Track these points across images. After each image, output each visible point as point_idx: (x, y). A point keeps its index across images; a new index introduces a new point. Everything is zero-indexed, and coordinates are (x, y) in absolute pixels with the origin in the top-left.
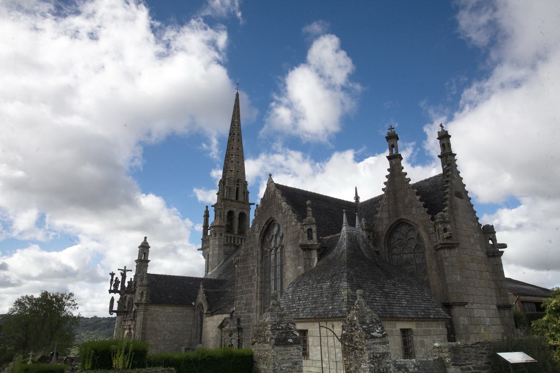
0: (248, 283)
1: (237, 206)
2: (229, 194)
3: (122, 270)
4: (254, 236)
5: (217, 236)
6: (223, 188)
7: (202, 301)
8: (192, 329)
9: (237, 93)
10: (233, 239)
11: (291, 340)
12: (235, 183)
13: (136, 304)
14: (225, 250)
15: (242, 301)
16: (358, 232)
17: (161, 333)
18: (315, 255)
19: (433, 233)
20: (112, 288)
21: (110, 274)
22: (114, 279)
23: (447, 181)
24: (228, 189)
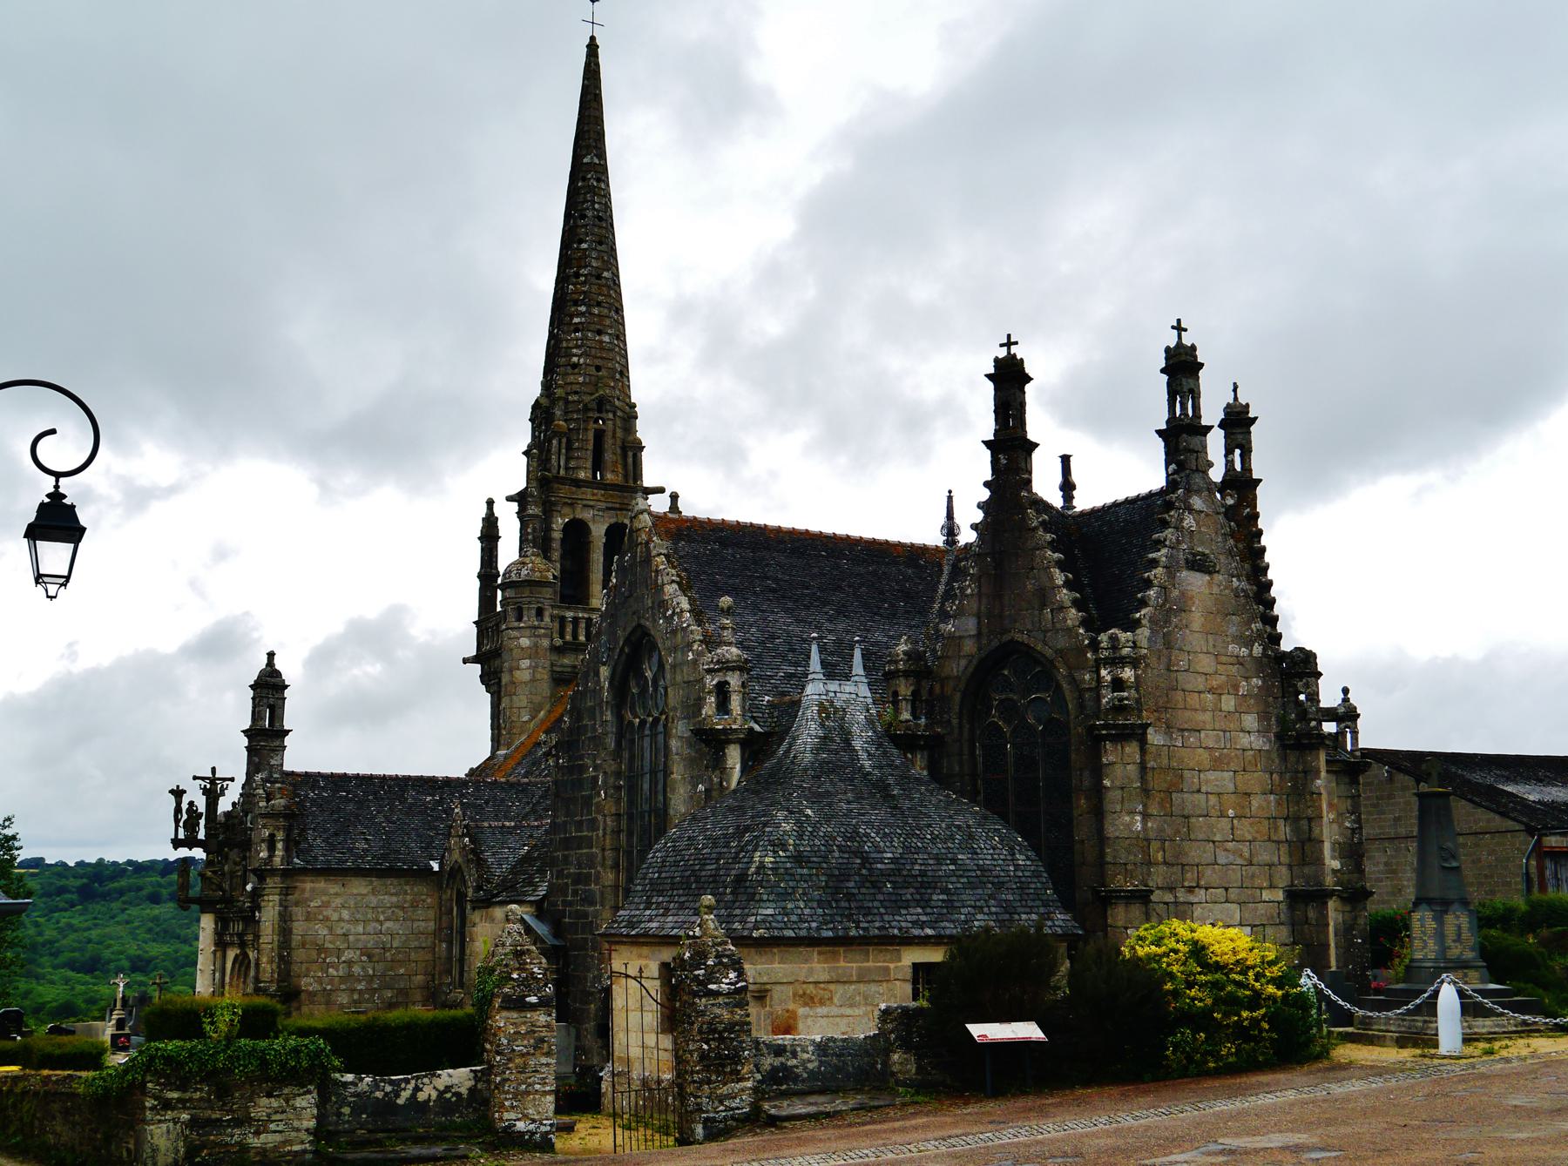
1: (599, 503)
2: (568, 459)
3: (203, 779)
4: (597, 674)
5: (525, 619)
6: (546, 431)
7: (460, 860)
8: (435, 943)
9: (593, 38)
11: (533, 999)
13: (254, 871)
14: (555, 668)
16: (854, 696)
17: (338, 958)
18: (734, 756)
19: (1090, 689)
20: (181, 835)
21: (172, 792)
22: (185, 806)
23: (1165, 524)
24: (564, 440)
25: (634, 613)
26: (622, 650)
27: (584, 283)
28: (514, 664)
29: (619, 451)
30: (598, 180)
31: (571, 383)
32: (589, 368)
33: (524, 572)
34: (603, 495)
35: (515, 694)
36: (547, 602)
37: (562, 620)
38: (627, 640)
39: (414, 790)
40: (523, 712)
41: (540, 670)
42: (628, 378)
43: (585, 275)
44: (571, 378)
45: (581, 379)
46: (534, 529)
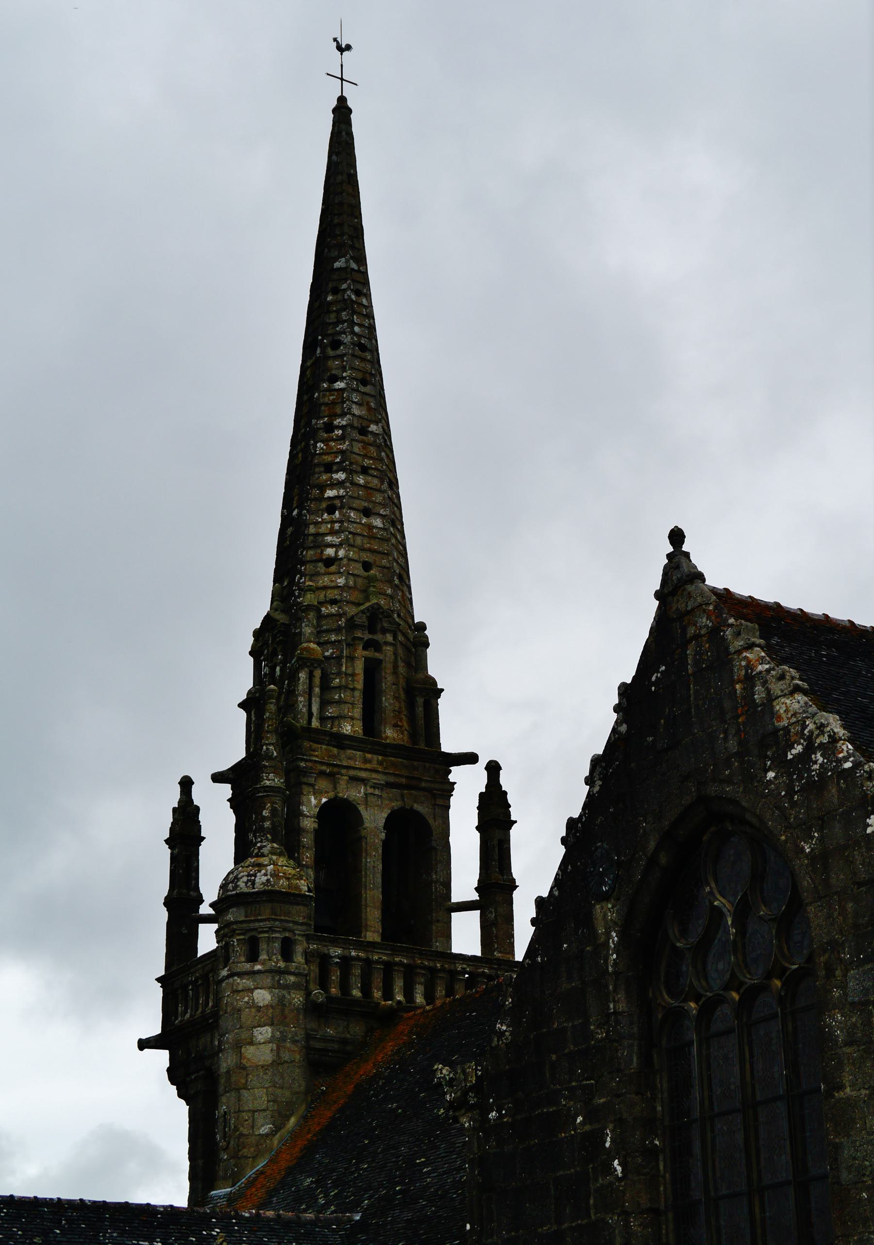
1: (374, 775)
2: (324, 703)
4: (588, 921)
5: (263, 957)
9: (342, 100)
24: (318, 673)
27: (342, 438)
28: (244, 1035)
29: (403, 696)
30: (358, 293)
31: (325, 588)
33: (261, 879)
34: (380, 763)
35: (246, 1088)
36: (299, 930)
37: (324, 960)
40: (260, 1118)
42: (409, 587)
43: (343, 428)
44: (325, 580)
45: (341, 581)
46: (274, 811)
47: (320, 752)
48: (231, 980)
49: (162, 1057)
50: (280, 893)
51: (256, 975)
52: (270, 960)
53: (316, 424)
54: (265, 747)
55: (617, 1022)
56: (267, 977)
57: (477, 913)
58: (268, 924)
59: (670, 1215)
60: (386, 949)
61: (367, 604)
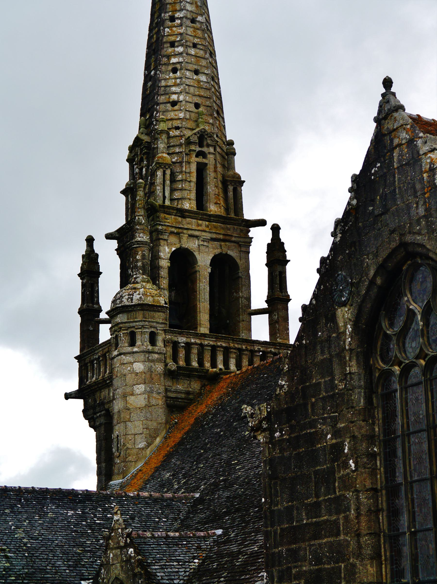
0: (317, 496)
1: (204, 234)
2: (172, 191)
4: (333, 319)
5: (138, 343)
6: (148, 166)
10: (195, 351)
12: (193, 147)
15: (295, 567)
24: (168, 172)
25: (392, 232)
26: (372, 282)
27: (181, 25)
28: (128, 390)
29: (220, 185)
31: (172, 119)
32: (189, 104)
33: (136, 297)
34: (207, 226)
37: (175, 345)
38: (381, 268)
39: (54, 504)
40: (138, 438)
41: (155, 395)
42: (223, 118)
43: (181, 18)
46: (143, 256)
47: (171, 220)
48: (119, 357)
49: (79, 404)
50: (148, 305)
51: (135, 354)
52: (142, 345)
53: (164, 16)
54: (137, 218)
55: (351, 379)
56: (141, 355)
57: (267, 315)
58: (141, 323)
59: (384, 492)
60: (212, 338)
61: (198, 129)
